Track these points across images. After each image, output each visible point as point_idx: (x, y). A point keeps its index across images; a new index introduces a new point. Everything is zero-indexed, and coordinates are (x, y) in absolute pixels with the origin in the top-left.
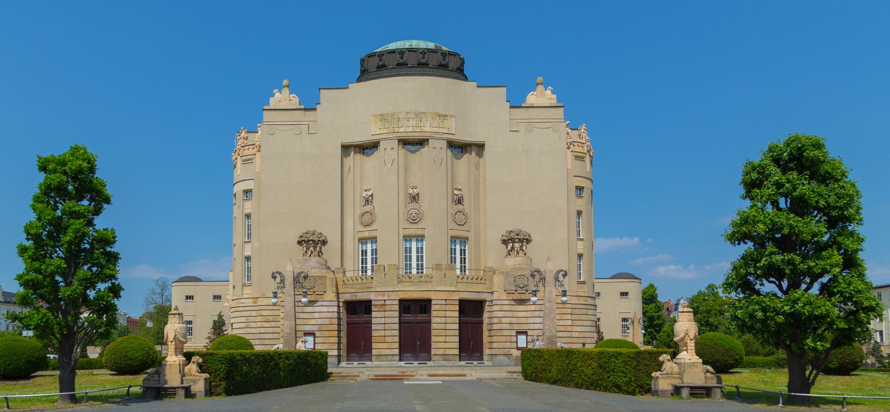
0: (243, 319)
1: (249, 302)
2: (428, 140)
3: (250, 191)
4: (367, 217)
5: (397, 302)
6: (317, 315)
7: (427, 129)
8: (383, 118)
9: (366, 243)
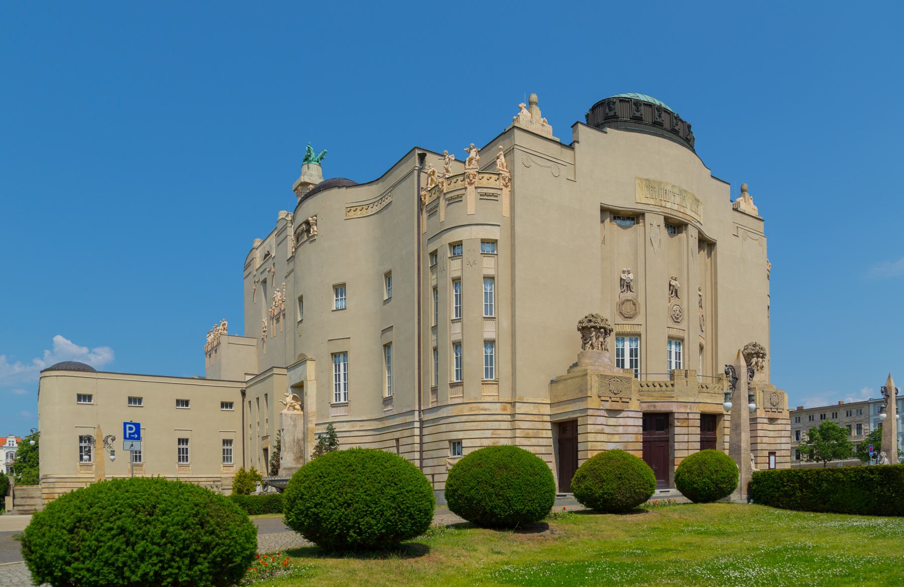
0: (488, 434)
2: (686, 225)
3: (494, 242)
4: (628, 308)
5: (698, 416)
7: (688, 212)
8: (650, 185)
9: (623, 340)
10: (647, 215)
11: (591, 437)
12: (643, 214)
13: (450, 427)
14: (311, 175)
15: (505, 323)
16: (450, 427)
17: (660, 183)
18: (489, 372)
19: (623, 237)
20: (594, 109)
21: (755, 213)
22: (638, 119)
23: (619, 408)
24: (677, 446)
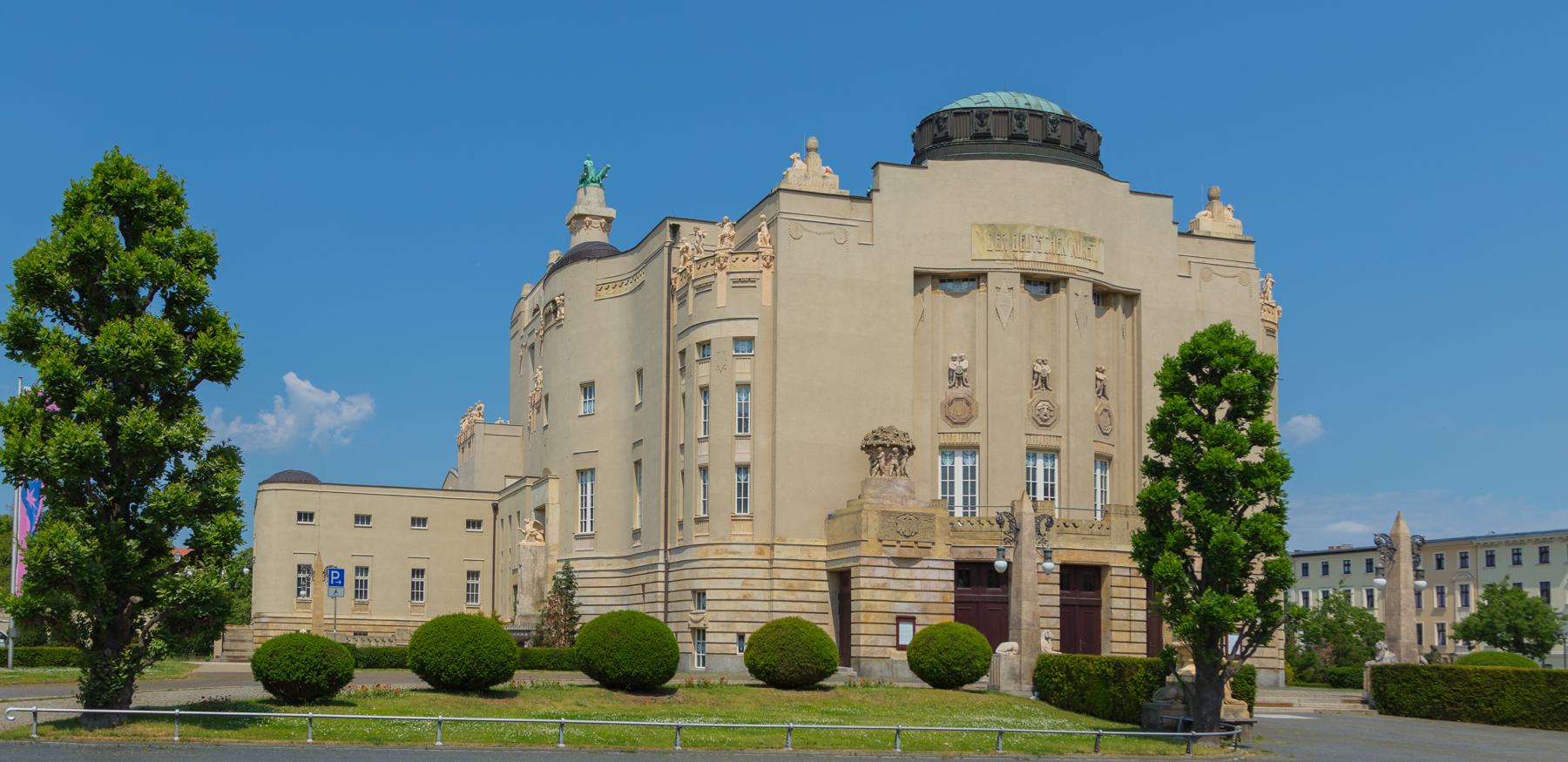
0: (738, 584)
1: (750, 552)
2: (1066, 280)
3: (751, 340)
4: (959, 410)
6: (917, 585)
7: (1068, 260)
11: (865, 594)
12: (985, 275)
13: (693, 574)
14: (589, 203)
15: (763, 442)
16: (693, 574)
17: (1013, 227)
18: (743, 505)
19: (952, 309)
20: (920, 128)
21: (1238, 232)
22: (981, 137)
23: (913, 555)
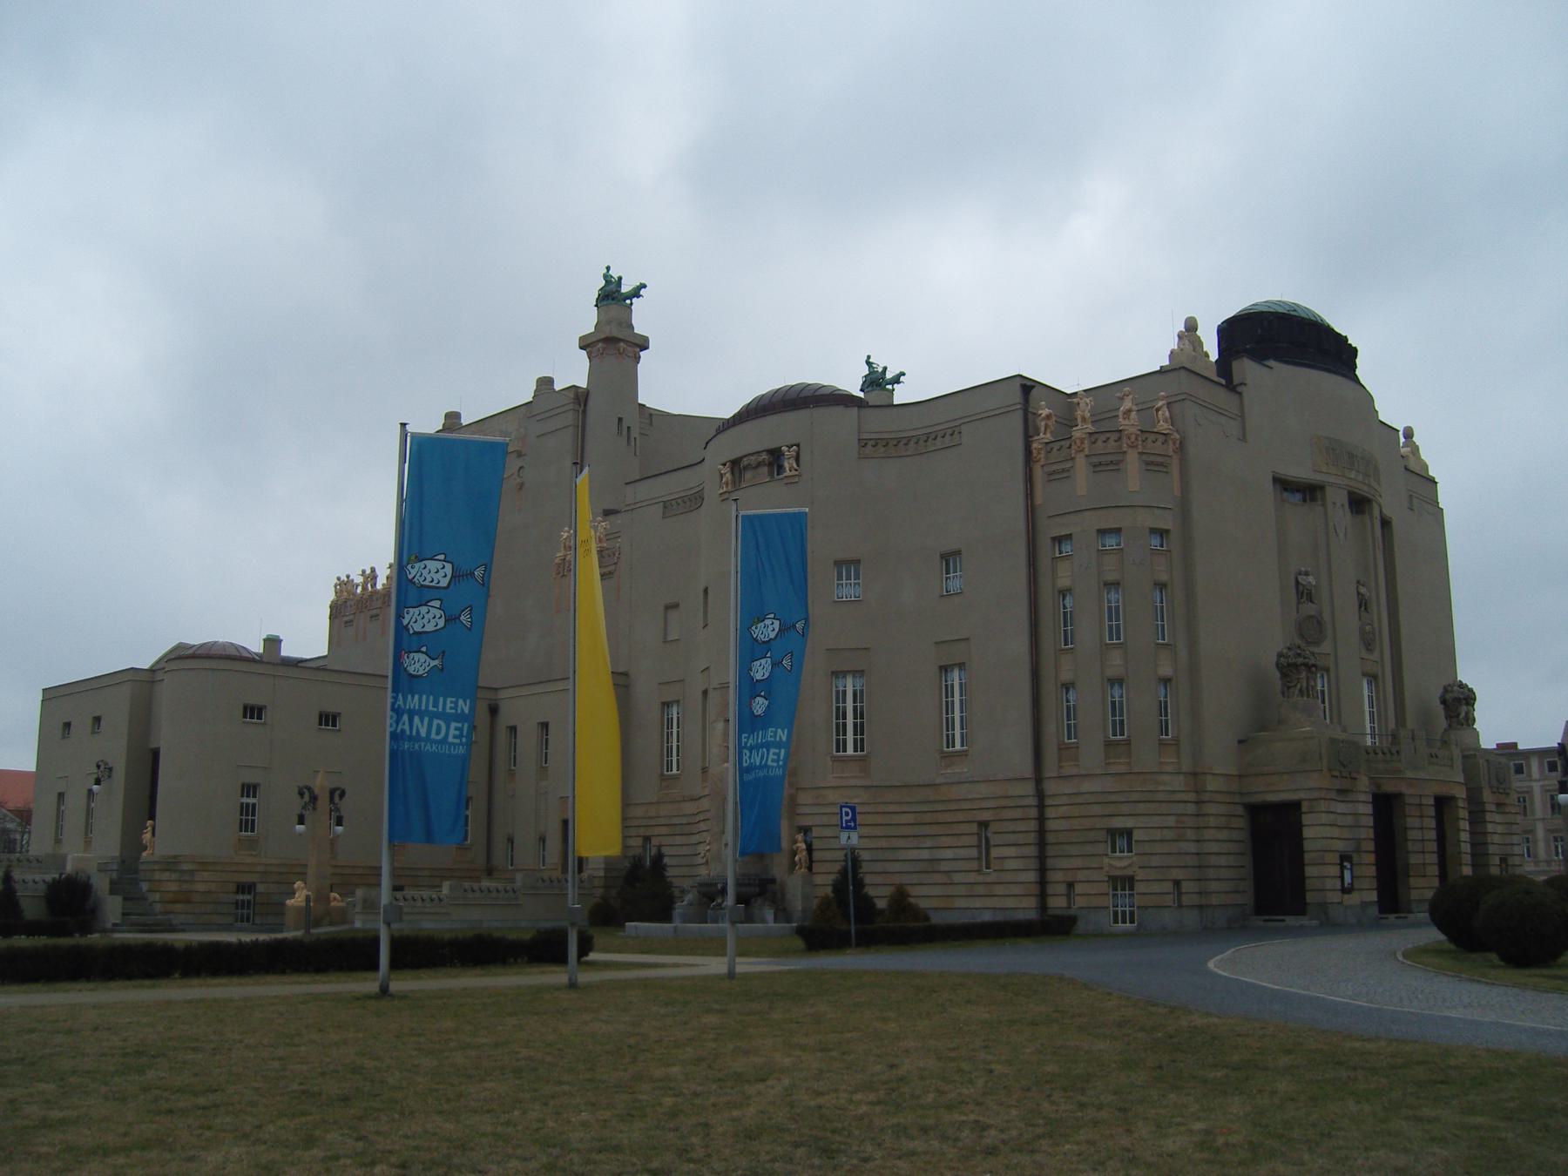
0: (1171, 821)
1: (1178, 783)
3: (1167, 531)
5: (1432, 801)
10: (1329, 491)
24: (1411, 846)
